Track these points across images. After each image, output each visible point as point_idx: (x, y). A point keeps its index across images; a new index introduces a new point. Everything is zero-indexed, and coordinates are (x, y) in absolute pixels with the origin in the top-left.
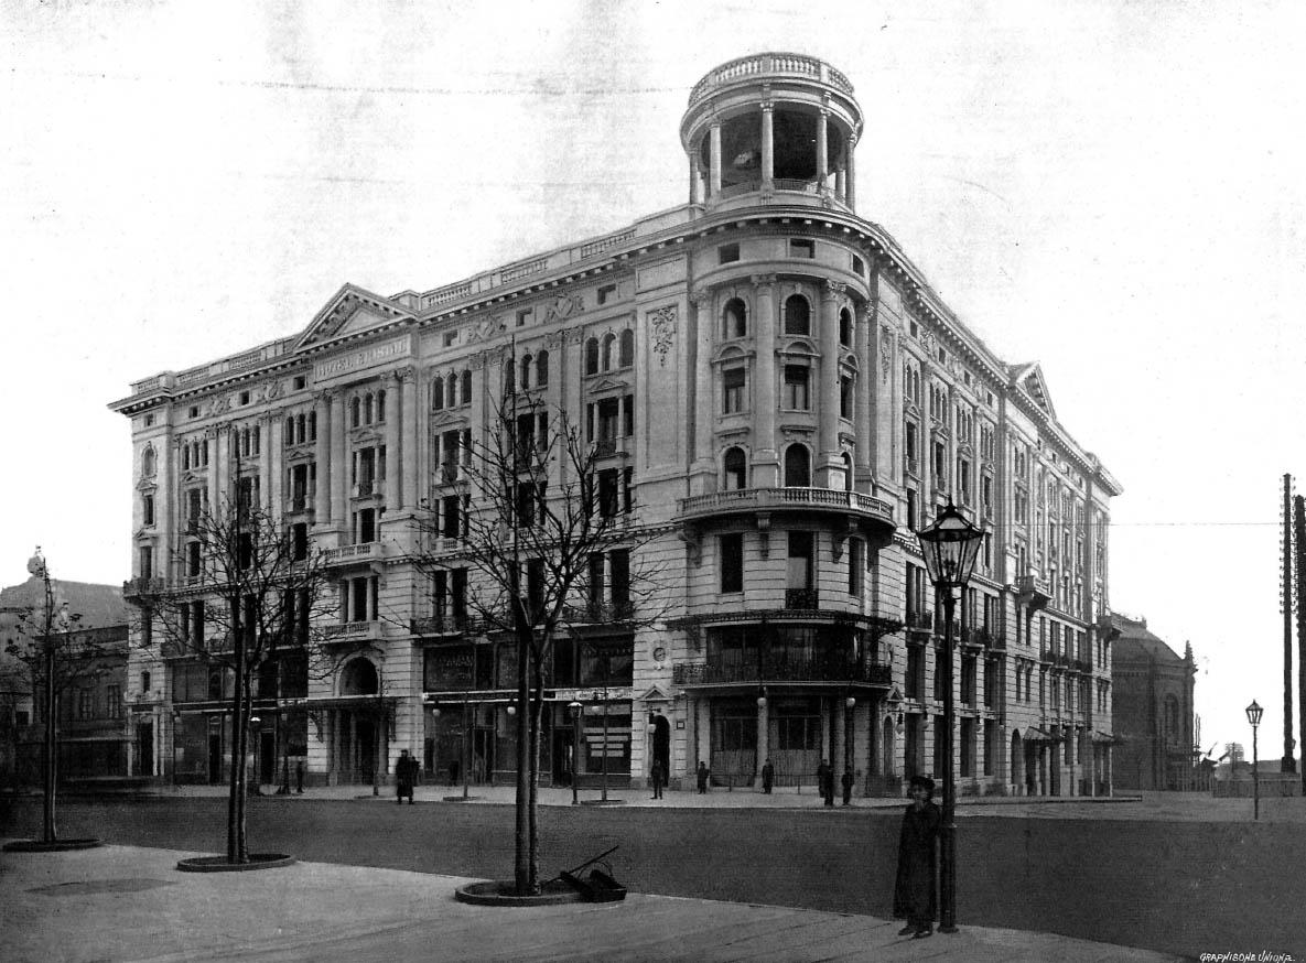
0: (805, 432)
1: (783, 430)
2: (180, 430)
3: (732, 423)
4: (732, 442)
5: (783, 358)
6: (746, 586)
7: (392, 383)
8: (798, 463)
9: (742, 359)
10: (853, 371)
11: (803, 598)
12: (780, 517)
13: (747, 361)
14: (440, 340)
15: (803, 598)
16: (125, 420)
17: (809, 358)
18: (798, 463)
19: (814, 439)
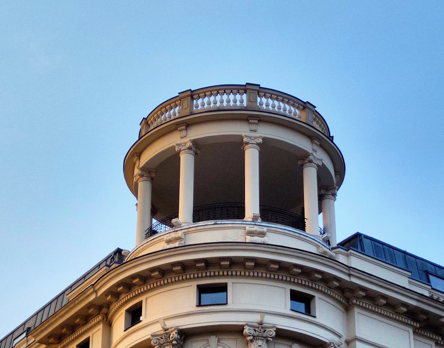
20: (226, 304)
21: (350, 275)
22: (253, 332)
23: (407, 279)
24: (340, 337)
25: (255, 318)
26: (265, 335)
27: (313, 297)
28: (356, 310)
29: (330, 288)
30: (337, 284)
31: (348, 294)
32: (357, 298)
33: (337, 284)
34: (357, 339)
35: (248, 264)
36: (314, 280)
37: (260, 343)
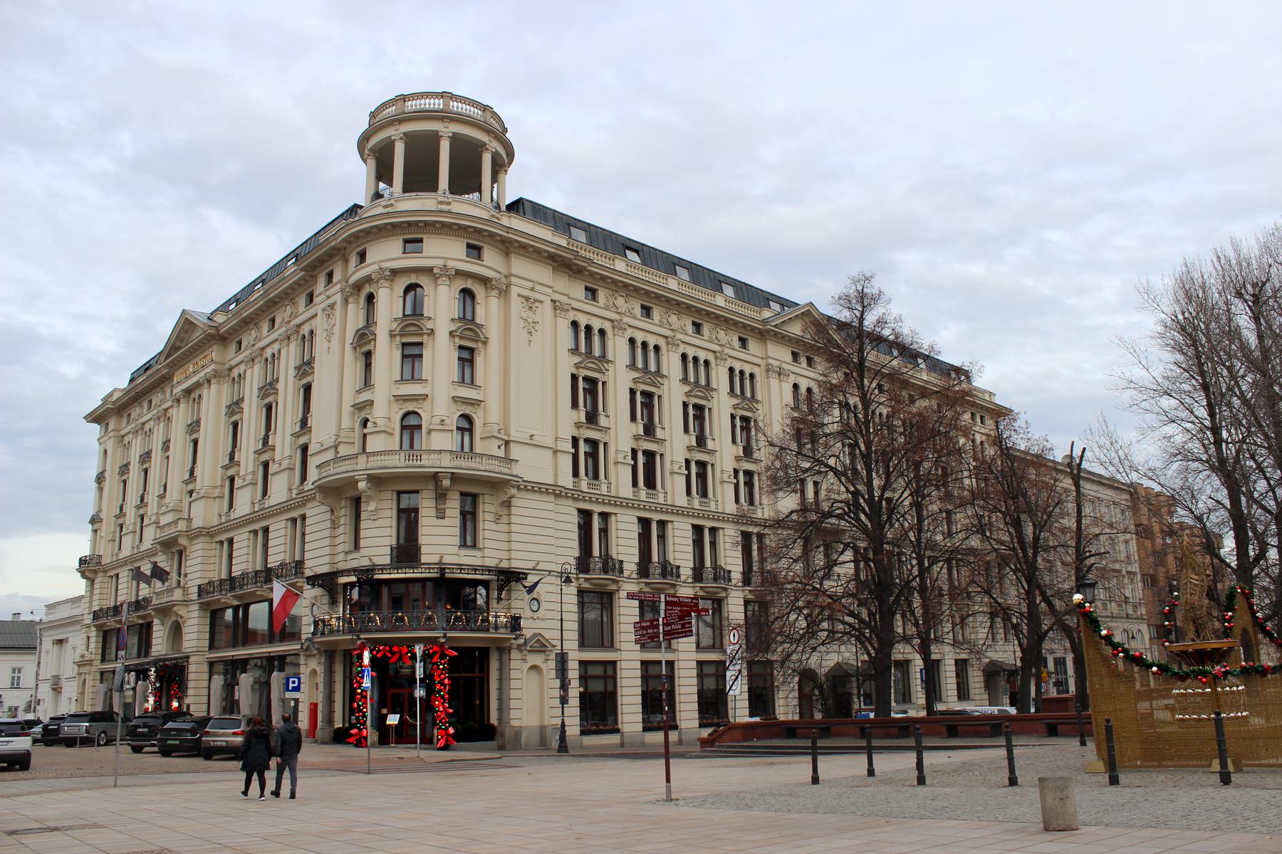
0: (417, 400)
1: (455, 399)
2: (123, 433)
3: (365, 396)
4: (363, 415)
5: (398, 338)
6: (363, 543)
7: (206, 385)
8: (410, 427)
9: (369, 342)
10: (476, 341)
11: (407, 551)
12: (378, 481)
13: (372, 343)
14: (233, 348)
15: (407, 551)
16: (96, 428)
17: (421, 335)
18: (410, 427)
19: (426, 405)
20: (421, 252)
21: (508, 232)
22: (439, 272)
23: (550, 233)
24: (500, 273)
25: (440, 263)
26: (448, 273)
27: (483, 247)
28: (513, 255)
29: (495, 241)
30: (499, 238)
31: (507, 245)
32: (514, 247)
33: (499, 238)
34: (511, 275)
35: (437, 225)
36: (484, 236)
37: (444, 279)
